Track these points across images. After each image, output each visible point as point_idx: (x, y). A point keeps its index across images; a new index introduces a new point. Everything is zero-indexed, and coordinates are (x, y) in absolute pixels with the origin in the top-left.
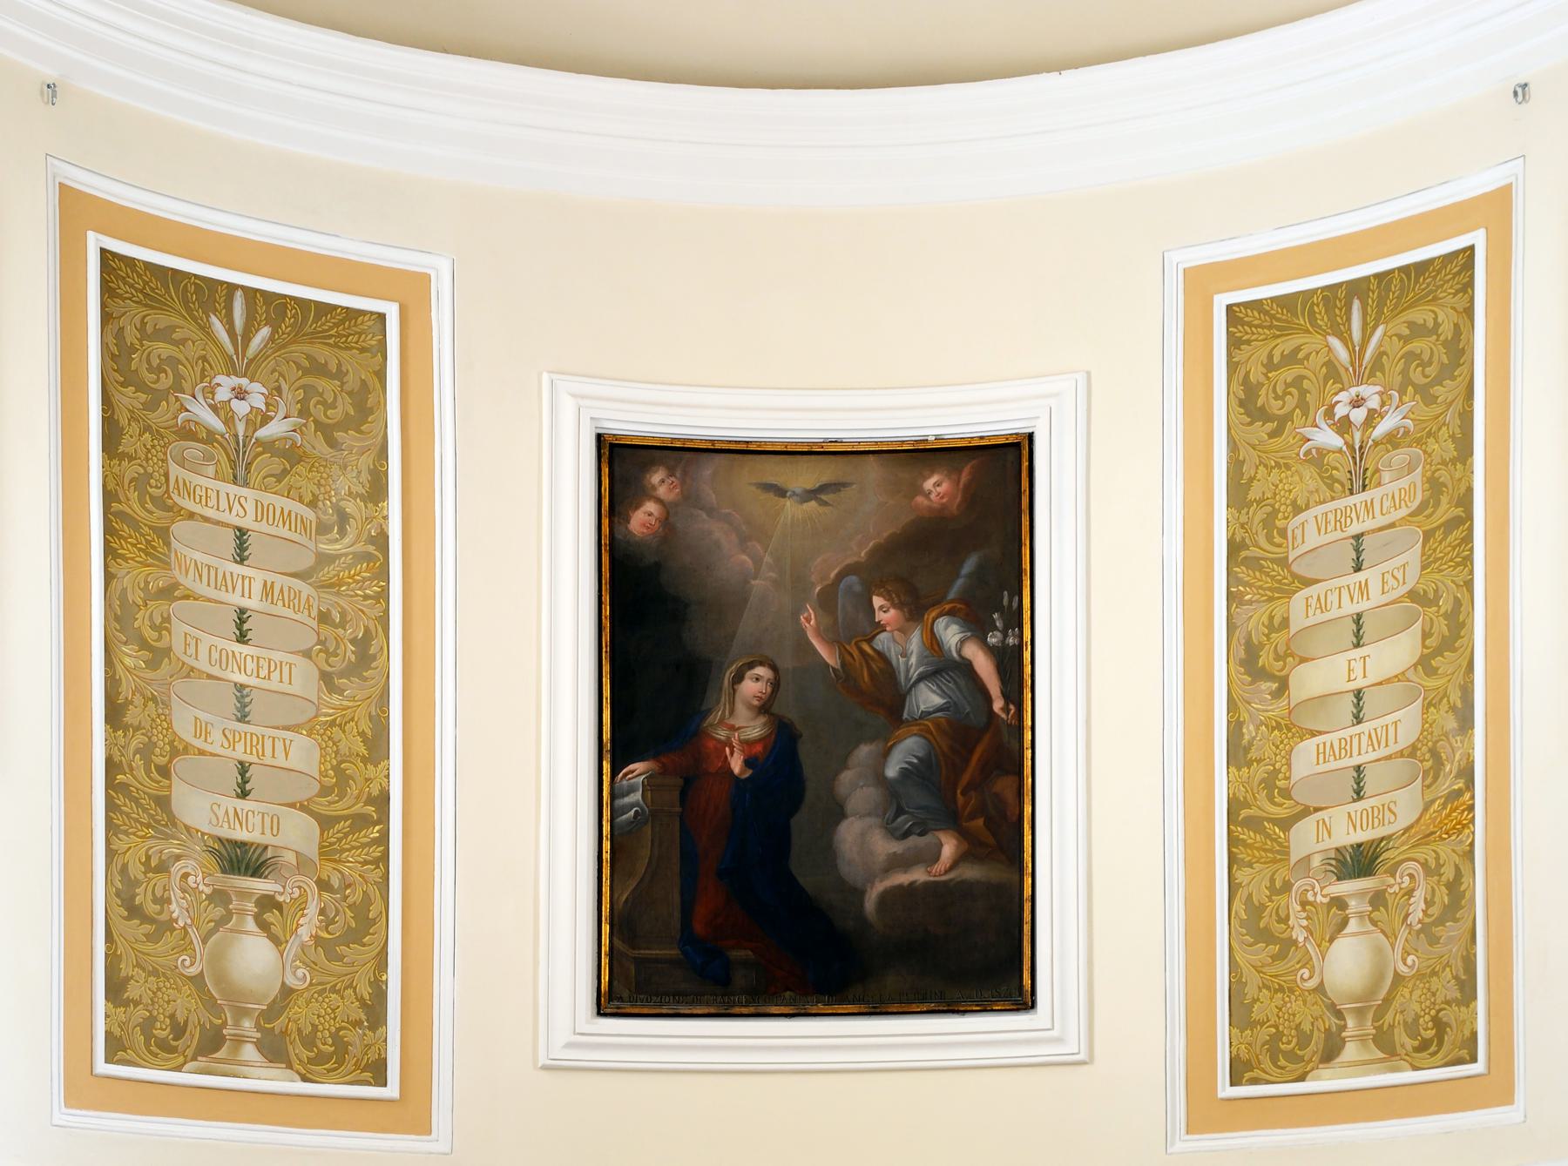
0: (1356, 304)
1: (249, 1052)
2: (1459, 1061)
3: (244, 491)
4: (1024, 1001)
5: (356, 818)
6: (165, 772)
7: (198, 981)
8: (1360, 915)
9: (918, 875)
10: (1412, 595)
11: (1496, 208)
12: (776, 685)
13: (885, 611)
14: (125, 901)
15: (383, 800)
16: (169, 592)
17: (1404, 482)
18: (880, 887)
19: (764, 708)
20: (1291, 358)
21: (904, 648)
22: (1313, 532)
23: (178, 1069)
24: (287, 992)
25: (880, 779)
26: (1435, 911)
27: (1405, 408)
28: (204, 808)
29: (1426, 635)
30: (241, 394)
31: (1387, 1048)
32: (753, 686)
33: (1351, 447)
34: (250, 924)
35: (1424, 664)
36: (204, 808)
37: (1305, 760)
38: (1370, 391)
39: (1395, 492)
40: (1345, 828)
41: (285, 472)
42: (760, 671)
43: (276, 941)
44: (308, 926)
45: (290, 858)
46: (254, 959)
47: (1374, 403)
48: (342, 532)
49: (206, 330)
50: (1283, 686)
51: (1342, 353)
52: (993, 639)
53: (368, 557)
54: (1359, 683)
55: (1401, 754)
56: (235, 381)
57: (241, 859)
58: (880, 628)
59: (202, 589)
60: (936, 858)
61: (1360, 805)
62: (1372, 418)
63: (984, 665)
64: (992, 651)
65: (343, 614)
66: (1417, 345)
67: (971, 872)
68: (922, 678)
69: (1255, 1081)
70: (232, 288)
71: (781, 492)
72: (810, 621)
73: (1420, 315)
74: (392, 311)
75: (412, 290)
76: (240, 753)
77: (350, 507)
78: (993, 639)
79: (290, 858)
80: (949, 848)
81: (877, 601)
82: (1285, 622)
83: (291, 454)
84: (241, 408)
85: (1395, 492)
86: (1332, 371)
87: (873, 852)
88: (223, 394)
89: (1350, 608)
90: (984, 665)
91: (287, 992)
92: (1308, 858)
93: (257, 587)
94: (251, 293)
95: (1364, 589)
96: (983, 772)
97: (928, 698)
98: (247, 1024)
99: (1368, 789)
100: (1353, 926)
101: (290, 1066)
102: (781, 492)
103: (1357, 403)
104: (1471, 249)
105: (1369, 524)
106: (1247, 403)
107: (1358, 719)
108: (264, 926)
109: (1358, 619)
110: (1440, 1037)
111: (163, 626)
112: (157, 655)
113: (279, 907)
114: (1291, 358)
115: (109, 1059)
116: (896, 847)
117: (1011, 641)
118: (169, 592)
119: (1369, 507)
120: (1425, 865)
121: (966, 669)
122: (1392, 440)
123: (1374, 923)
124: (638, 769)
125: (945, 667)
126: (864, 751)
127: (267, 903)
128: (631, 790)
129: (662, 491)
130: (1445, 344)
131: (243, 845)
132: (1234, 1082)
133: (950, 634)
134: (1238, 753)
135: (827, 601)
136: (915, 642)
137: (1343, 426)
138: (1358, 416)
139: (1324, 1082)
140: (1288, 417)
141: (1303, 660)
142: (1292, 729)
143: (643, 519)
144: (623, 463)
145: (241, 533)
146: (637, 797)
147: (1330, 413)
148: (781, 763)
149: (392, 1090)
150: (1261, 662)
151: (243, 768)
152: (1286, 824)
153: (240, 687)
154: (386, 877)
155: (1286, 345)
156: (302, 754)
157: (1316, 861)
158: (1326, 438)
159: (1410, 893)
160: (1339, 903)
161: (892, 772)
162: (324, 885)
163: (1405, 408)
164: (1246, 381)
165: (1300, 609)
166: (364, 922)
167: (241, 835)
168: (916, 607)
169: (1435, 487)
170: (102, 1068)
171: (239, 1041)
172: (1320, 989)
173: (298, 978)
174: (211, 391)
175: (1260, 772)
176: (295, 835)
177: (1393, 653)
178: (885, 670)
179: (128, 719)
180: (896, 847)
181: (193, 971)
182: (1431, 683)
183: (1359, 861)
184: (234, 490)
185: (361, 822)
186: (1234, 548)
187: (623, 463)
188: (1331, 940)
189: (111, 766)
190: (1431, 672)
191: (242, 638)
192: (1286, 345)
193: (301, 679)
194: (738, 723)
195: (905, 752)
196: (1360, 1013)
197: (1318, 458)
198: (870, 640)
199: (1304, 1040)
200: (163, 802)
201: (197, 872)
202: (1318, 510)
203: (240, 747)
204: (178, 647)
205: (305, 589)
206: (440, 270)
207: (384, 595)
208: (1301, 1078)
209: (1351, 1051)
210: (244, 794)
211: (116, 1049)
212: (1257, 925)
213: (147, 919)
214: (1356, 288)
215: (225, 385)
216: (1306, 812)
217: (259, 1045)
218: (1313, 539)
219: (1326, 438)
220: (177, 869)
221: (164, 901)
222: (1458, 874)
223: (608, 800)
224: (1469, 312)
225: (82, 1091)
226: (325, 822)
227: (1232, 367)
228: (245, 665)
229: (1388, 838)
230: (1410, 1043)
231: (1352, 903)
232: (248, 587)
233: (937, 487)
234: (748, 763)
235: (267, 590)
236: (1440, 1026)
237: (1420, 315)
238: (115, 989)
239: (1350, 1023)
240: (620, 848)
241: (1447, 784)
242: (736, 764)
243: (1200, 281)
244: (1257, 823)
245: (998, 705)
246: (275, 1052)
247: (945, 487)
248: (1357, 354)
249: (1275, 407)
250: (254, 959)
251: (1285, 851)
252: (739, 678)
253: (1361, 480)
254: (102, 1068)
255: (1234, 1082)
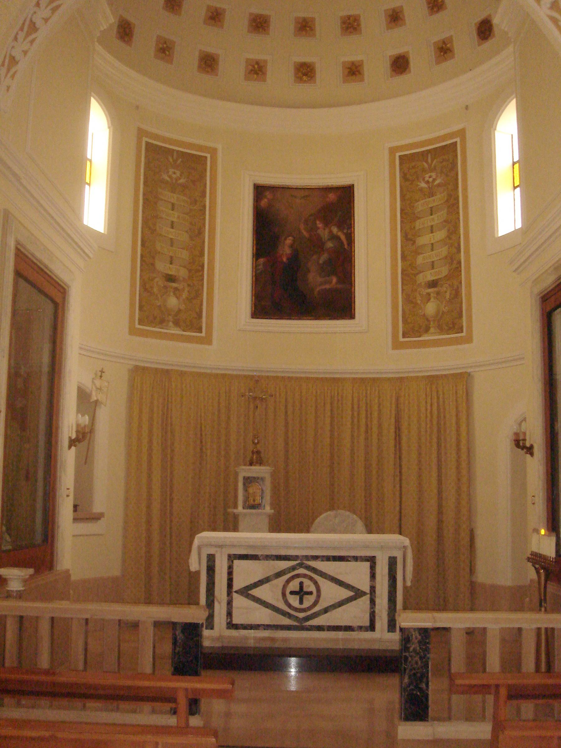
0: (429, 155)
1: (171, 324)
2: (459, 333)
3: (174, 195)
4: (352, 316)
5: (197, 269)
6: (154, 258)
7: (160, 306)
8: (434, 297)
9: (327, 286)
10: (445, 221)
11: (462, 133)
12: (294, 241)
13: (319, 225)
14: (144, 285)
15: (203, 266)
16: (156, 217)
17: (442, 195)
18: (318, 289)
19: (291, 246)
20: (413, 167)
21: (324, 233)
22: (421, 206)
23: (155, 327)
24: (180, 310)
25: (318, 264)
26: (452, 296)
27: (442, 178)
28: (162, 266)
29: (448, 230)
30: (174, 173)
31: (441, 330)
32: (289, 241)
33: (429, 187)
34: (172, 294)
35: (449, 237)
36: (162, 266)
37: (420, 260)
38: (433, 175)
39: (439, 199)
40: (430, 276)
41: (184, 191)
42: (290, 238)
43: (177, 298)
44: (185, 295)
45: (181, 279)
46: (173, 302)
47: (434, 177)
48: (196, 204)
49: (167, 159)
50: (414, 242)
51: (426, 165)
52: (345, 231)
53: (201, 210)
54: (432, 242)
55: (443, 258)
56: (173, 170)
57: (170, 279)
58: (319, 228)
59: (164, 216)
60: (331, 282)
61: (433, 271)
62: (434, 180)
63: (343, 237)
64: (344, 234)
65: (195, 223)
66: (444, 163)
67: (339, 286)
68: (329, 240)
69: (409, 337)
70: (174, 150)
71: (295, 197)
72: (302, 227)
73: (446, 157)
74: (208, 156)
75: (214, 151)
76: (171, 254)
77: (198, 199)
78: (345, 231)
79: (181, 279)
80: (334, 280)
81: (318, 222)
82: (414, 227)
83: (184, 186)
84: (174, 176)
85: (439, 199)
86: (424, 170)
87: (317, 281)
88: (170, 173)
89: (430, 224)
90: (343, 237)
91: (180, 310)
92: (421, 283)
93: (176, 216)
94: (178, 151)
95: (433, 219)
96: (342, 262)
97: (330, 245)
98: (170, 317)
99: (435, 267)
100: (432, 299)
101: (180, 328)
102: (295, 197)
103: (430, 177)
104: (456, 142)
105: (435, 204)
106: (404, 177)
107: (432, 250)
108: (174, 294)
109: (432, 226)
110: (454, 327)
111: (155, 225)
112: (153, 231)
113: (179, 290)
114: (413, 167)
115: (139, 324)
116: (322, 280)
117: (349, 232)
118: (156, 217)
119: (434, 200)
120: (449, 285)
121: (338, 238)
122: (439, 185)
123: (437, 299)
124: (262, 260)
125: (334, 237)
126: (315, 257)
127: (176, 289)
128: (259, 265)
129: (269, 197)
130: (451, 163)
131: (171, 275)
132: (404, 337)
133: (335, 230)
134: (404, 258)
135: (306, 222)
136: (327, 231)
137: (428, 182)
138: (431, 180)
139: (425, 338)
140: (413, 181)
141: (420, 236)
142: (417, 253)
143: (264, 203)
144: (260, 190)
145: (173, 205)
146: (261, 267)
147: (424, 179)
148: (295, 258)
149: (203, 334)
150: (409, 237)
151: (171, 258)
152: (416, 275)
153: (171, 239)
154: (203, 283)
155: (413, 164)
156: (185, 255)
157: (423, 284)
158: (423, 185)
159: (446, 292)
160: (429, 294)
161: (321, 262)
162: (189, 285)
163: (442, 178)
164: (404, 173)
165: (418, 224)
166: (198, 294)
167: (170, 273)
168: (327, 224)
169: (450, 196)
170: (138, 326)
171: (169, 321)
172: (424, 315)
173: (183, 307)
174: (168, 172)
175: (409, 263)
176: (183, 273)
177: (441, 235)
178: (319, 237)
179: (146, 245)
180: (322, 280)
181: (158, 304)
182: (451, 241)
183: (433, 284)
184: (172, 194)
185: (197, 271)
186: (402, 210)
187: (260, 190)
188: (427, 303)
189: (142, 256)
190: (450, 239)
191: (172, 228)
192: (413, 164)
193: (184, 237)
194: (285, 249)
195: (324, 257)
196: (434, 321)
197: (421, 190)
198: (316, 231)
199: (420, 327)
200: (153, 264)
201: (160, 282)
202: (422, 202)
203: (171, 253)
204: (158, 229)
205: (187, 217)
206: (219, 147)
207: (204, 219)
208: (420, 337)
209: (432, 330)
210: (171, 264)
211: (141, 322)
212: (409, 299)
213: (148, 292)
214: (429, 151)
215: (171, 171)
216: (420, 272)
217: (173, 323)
218: (420, 208)
219: (423, 185)
220: (156, 280)
221: (152, 287)
222: (458, 288)
223: (255, 267)
224: (456, 156)
225: (133, 331)
226: (190, 271)
227: (400, 169)
228: (172, 234)
229: (440, 279)
230: (446, 328)
231: (432, 294)
232: (174, 216)
233: (332, 197)
234: (288, 259)
235: (178, 217)
236: (454, 324)
237: (446, 157)
238: (141, 308)
239: (432, 323)
240: (257, 279)
241: (454, 266)
242: (285, 260)
243: (392, 151)
244: (409, 274)
245: (346, 246)
246: (177, 324)
247: (333, 197)
248: (430, 166)
249: (410, 178)
250: (173, 302)
251: (416, 281)
252: (285, 239)
253: (432, 194)
254: (138, 326)
255: (404, 337)
